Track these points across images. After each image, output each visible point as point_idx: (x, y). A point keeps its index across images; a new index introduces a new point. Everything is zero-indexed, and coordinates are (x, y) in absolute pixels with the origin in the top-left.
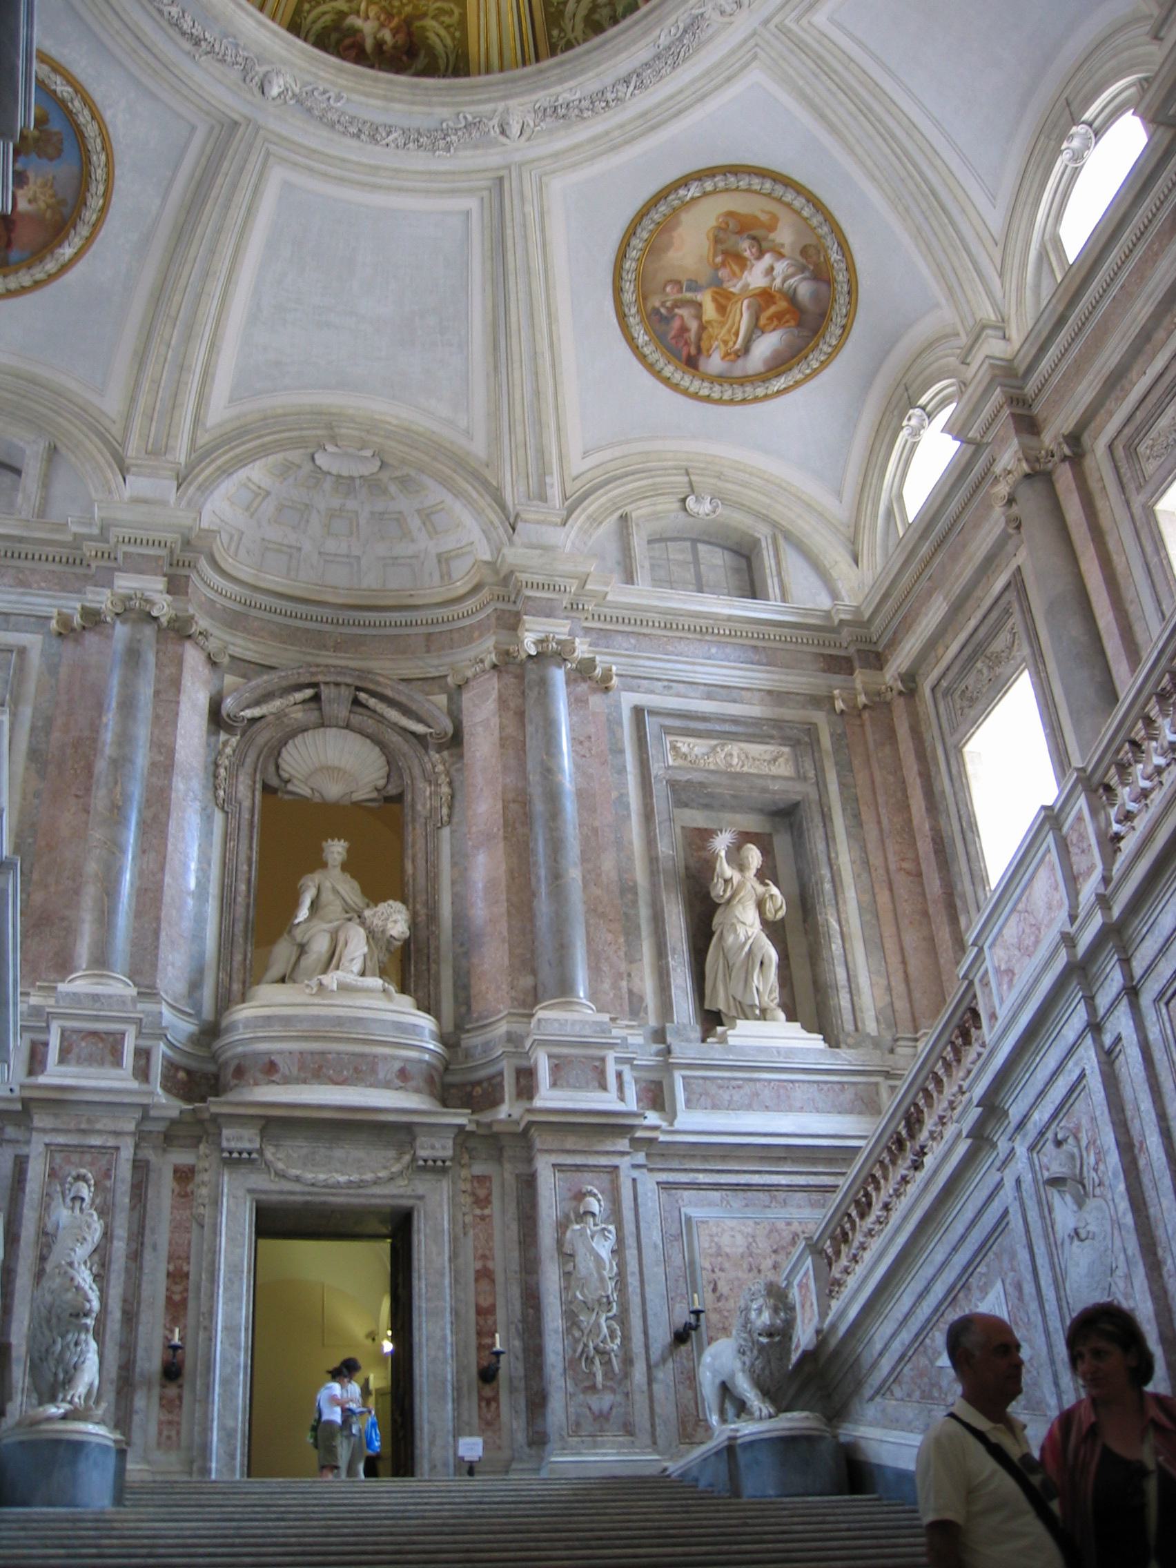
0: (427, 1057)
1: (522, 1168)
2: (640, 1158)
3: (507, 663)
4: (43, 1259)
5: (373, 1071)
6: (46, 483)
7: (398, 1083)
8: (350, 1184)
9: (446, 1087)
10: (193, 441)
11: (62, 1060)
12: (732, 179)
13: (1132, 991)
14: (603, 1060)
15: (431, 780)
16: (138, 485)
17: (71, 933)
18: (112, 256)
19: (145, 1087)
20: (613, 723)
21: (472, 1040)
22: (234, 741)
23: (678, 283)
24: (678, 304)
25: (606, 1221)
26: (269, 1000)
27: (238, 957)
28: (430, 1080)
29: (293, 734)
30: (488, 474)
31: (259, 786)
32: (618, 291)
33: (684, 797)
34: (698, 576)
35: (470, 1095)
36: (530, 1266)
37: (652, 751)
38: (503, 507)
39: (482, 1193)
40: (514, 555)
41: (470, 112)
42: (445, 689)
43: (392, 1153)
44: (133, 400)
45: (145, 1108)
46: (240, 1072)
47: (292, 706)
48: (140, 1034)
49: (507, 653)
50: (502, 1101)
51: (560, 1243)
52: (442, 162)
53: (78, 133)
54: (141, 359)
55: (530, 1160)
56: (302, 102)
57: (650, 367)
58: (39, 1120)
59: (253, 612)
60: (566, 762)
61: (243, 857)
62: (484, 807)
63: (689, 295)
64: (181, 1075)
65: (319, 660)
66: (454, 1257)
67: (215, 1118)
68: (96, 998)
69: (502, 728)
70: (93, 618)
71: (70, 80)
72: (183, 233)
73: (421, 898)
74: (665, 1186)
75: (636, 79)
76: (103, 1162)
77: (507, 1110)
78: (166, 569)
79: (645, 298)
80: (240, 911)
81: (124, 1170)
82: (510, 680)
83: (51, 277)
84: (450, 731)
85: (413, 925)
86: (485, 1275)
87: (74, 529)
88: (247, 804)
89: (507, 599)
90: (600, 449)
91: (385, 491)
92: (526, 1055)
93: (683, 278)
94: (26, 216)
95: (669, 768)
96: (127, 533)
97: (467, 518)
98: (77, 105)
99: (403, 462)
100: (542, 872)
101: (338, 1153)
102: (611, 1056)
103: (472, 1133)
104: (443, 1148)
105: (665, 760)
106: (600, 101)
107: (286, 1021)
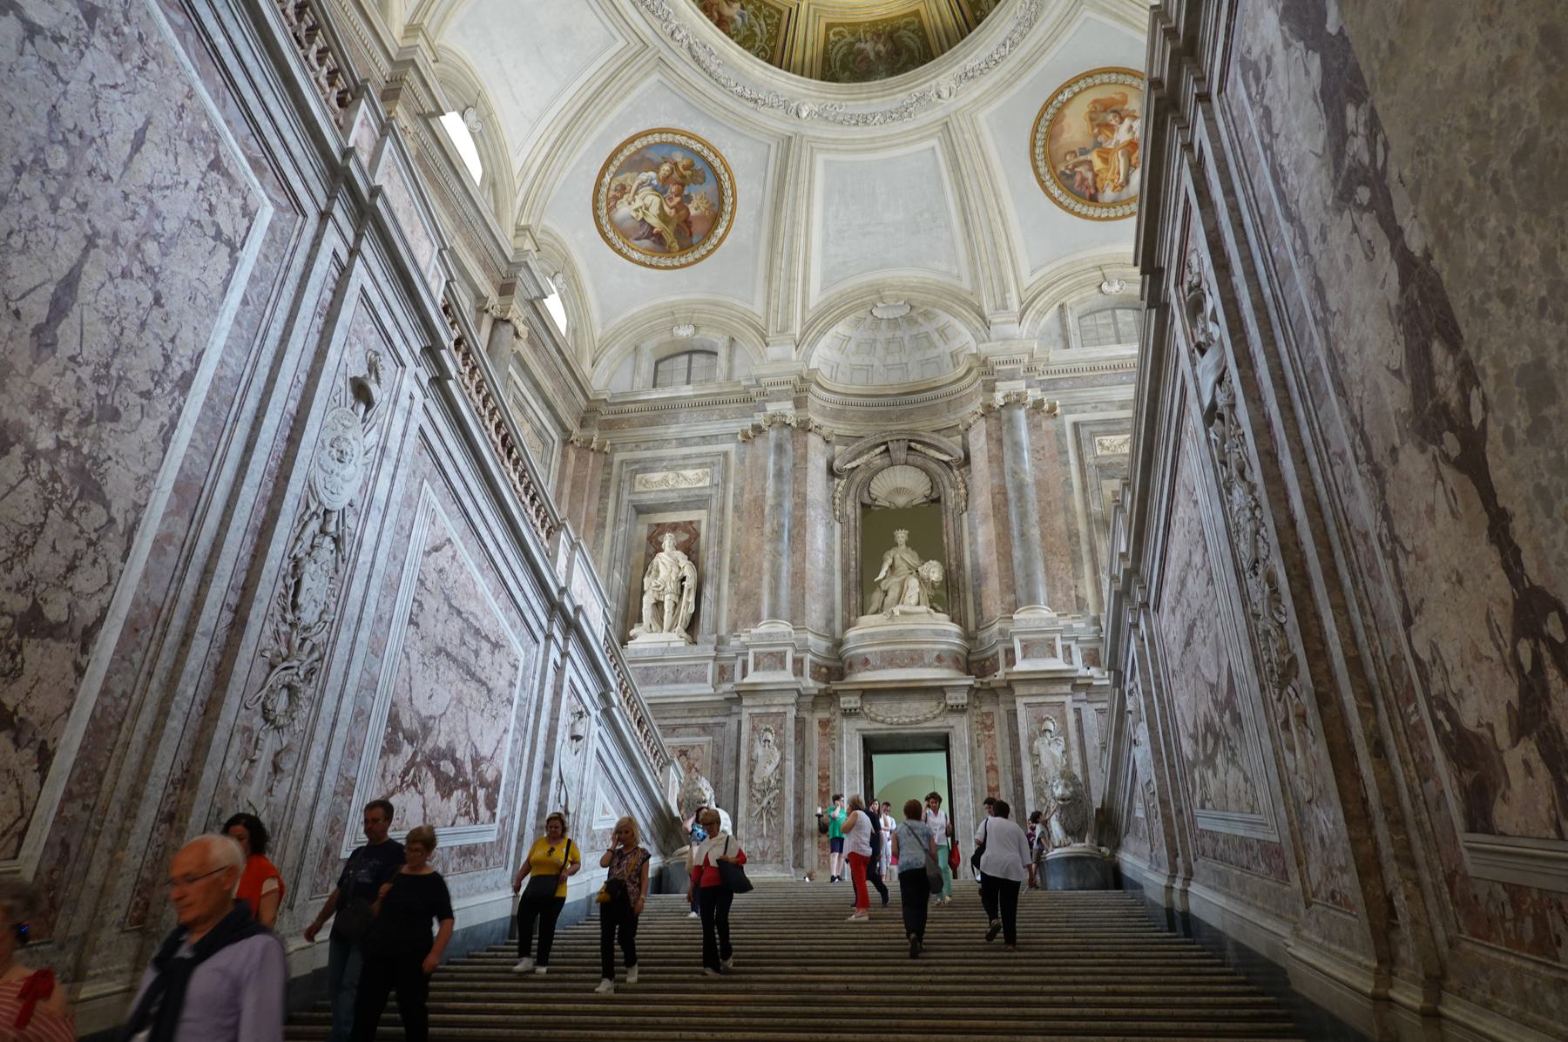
1: (1010, 707)
2: (1083, 695)
3: (989, 411)
4: (752, 773)
5: (922, 659)
6: (730, 359)
8: (911, 723)
11: (755, 669)
12: (1089, 80)
15: (954, 487)
16: (773, 352)
17: (759, 601)
20: (1060, 435)
21: (985, 635)
24: (1075, 166)
25: (1059, 734)
26: (868, 624)
28: (956, 661)
29: (877, 472)
30: (971, 298)
32: (1036, 168)
36: (1016, 763)
37: (1086, 448)
38: (983, 318)
39: (988, 722)
40: (985, 348)
41: (917, 91)
42: (959, 433)
43: (934, 703)
44: (768, 303)
46: (851, 666)
47: (875, 458)
51: (1031, 748)
52: (909, 125)
53: (710, 165)
54: (769, 279)
56: (821, 116)
57: (1066, 208)
60: (1027, 466)
62: (982, 500)
66: (972, 759)
67: (836, 692)
68: (770, 635)
69: (989, 451)
70: (758, 429)
71: (699, 140)
72: (777, 206)
73: (953, 556)
74: (1100, 711)
75: (1011, 43)
76: (779, 721)
77: (1000, 674)
80: (852, 576)
81: (790, 724)
82: (992, 421)
83: (716, 247)
85: (947, 574)
86: (992, 769)
90: (1041, 267)
92: (1011, 641)
97: (962, 328)
98: (706, 152)
99: (923, 303)
100: (1015, 533)
101: (905, 706)
102: (1058, 637)
103: (978, 690)
104: (962, 699)
106: (993, 62)
107: (872, 635)
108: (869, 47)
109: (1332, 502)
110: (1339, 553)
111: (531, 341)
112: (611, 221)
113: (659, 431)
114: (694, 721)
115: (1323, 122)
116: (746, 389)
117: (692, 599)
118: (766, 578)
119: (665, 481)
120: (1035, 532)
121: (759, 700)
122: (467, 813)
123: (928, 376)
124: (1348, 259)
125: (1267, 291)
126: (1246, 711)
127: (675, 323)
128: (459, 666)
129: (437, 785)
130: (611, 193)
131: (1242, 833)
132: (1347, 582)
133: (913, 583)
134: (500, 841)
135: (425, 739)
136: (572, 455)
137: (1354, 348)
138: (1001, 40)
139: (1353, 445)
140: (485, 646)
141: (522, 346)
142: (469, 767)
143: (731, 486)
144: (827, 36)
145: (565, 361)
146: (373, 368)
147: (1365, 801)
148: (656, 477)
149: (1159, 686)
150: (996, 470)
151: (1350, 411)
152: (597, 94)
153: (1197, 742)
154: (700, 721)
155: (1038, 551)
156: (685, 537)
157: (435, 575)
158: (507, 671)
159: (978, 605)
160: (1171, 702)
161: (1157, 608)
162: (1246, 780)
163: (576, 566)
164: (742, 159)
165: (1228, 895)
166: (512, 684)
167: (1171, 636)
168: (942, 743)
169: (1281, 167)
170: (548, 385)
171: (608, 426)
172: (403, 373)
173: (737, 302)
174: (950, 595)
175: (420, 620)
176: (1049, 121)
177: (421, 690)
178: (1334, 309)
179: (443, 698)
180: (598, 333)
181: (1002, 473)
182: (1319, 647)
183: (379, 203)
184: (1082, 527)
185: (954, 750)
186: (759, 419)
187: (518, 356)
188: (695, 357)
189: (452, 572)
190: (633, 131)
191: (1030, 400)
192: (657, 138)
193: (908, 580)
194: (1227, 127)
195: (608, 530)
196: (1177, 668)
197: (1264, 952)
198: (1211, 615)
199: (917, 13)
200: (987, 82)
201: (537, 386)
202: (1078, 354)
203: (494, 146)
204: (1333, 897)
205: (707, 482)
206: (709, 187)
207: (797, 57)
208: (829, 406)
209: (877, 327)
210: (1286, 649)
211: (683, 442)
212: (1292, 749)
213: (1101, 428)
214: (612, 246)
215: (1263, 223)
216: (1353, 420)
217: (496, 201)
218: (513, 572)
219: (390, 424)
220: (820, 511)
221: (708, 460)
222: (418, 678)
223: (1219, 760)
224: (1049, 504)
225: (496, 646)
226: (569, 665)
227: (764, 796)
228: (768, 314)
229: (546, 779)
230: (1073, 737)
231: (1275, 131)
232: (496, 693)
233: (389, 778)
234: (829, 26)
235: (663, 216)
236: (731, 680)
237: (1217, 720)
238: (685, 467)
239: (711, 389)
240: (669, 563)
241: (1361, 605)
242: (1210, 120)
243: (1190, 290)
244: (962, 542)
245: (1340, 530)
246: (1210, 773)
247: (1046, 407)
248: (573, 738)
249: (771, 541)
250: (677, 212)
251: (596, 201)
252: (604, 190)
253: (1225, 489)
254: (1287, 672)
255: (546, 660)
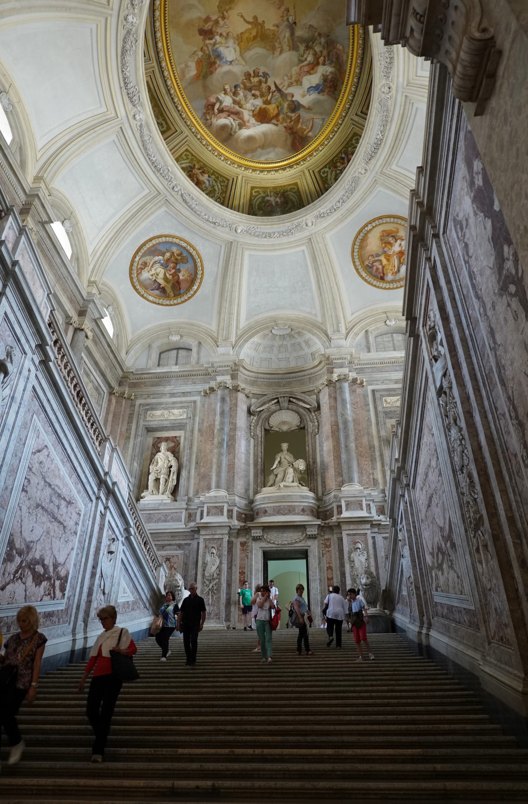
0: (311, 505)
1: (339, 536)
2: (376, 530)
3: (330, 383)
4: (204, 570)
5: (294, 510)
6: (198, 353)
7: (302, 513)
9: (318, 513)
10: (236, 333)
12: (380, 221)
13: (408, 485)
14: (362, 501)
16: (221, 350)
17: (210, 479)
18: (207, 286)
19: (231, 520)
20: (365, 396)
21: (326, 498)
22: (255, 418)
23: (372, 255)
24: (373, 262)
25: (364, 550)
26: (267, 492)
27: (259, 480)
30: (321, 326)
31: (263, 430)
32: (354, 262)
33: (390, 416)
34: (394, 345)
35: (326, 514)
36: (342, 565)
37: (378, 403)
38: (327, 336)
39: (328, 544)
40: (328, 351)
42: (315, 394)
43: (300, 534)
44: (219, 325)
45: (229, 526)
46: (257, 514)
47: (272, 406)
48: (229, 506)
49: (330, 381)
50: (333, 516)
52: (292, 238)
53: (191, 254)
54: (220, 313)
55: (341, 533)
57: (369, 283)
58: (202, 532)
59: (259, 380)
60: (349, 412)
61: (259, 451)
62: (326, 428)
63: (377, 258)
64: (243, 516)
65: (279, 391)
66: (319, 563)
68: (216, 497)
69: (330, 403)
70: (212, 390)
71: (185, 242)
73: (311, 457)
77: (334, 519)
78: (231, 372)
79: (363, 263)
80: (259, 467)
81: (225, 545)
82: (332, 388)
83: (193, 295)
84: (316, 406)
85: (308, 466)
86: (330, 568)
87: (205, 366)
88: (260, 436)
89: (329, 364)
90: (357, 311)
91: (294, 337)
92: (340, 501)
93: (374, 254)
94: (183, 280)
95: (384, 408)
96: (219, 364)
98: (189, 248)
100: (343, 446)
101: (285, 535)
102: (364, 499)
103: (323, 527)
104: (313, 531)
105: (382, 404)
106: (334, 210)
107: (269, 498)
108: (272, 199)
109: (499, 439)
110: (503, 464)
111: (94, 341)
112: (138, 280)
113: (160, 389)
114: (174, 542)
115: (493, 252)
116: (207, 369)
117: (175, 477)
118: (214, 467)
119: (163, 415)
120: (353, 445)
121: (209, 532)
122: (49, 594)
123: (299, 364)
124: (505, 320)
125: (467, 332)
126: (458, 541)
127: (170, 334)
128: (48, 514)
129: (33, 579)
130: (139, 266)
131: (456, 605)
132: (507, 479)
133: (291, 470)
134: (67, 609)
135: (28, 553)
136: (114, 401)
137: (509, 363)
138: (337, 199)
139: (509, 411)
140: (63, 503)
141: (89, 343)
142: (51, 569)
143: (197, 419)
144: (251, 193)
145: (112, 351)
146: (9, 355)
147: (517, 590)
148: (158, 413)
149: (415, 527)
150: (333, 413)
151: (508, 394)
152: (134, 216)
153: (433, 557)
154: (177, 542)
155: (354, 455)
156: (172, 444)
157: (37, 465)
158: (75, 516)
159: (324, 482)
160: (421, 535)
161: (414, 487)
162: (458, 577)
163: (114, 461)
164: (208, 253)
165: (450, 637)
166: (77, 524)
167: (421, 502)
168: (304, 554)
169: (473, 272)
170: (102, 364)
171: (134, 385)
172: (25, 357)
173: (203, 324)
174: (309, 477)
175: (28, 489)
176: (360, 240)
177: (27, 526)
178: (499, 343)
179: (39, 531)
180: (130, 337)
181: (336, 415)
182: (494, 511)
183: (17, 269)
184: (376, 443)
185: (309, 558)
186: (213, 384)
187: (87, 349)
188: (180, 351)
189: (47, 464)
190: (151, 235)
191: (351, 378)
192: (164, 239)
193: (288, 470)
194: (447, 251)
195: (132, 440)
196: (423, 518)
197: (468, 668)
198: (441, 492)
199: (296, 184)
200: (330, 220)
201: (96, 364)
202: (374, 355)
203: (78, 239)
204: (502, 640)
205: (185, 416)
206: (190, 265)
207: (236, 202)
208: (249, 378)
209: (274, 339)
210: (477, 511)
211: (173, 395)
212: (481, 562)
213: (386, 393)
214: (139, 293)
215: (465, 298)
216: (509, 398)
217: (78, 268)
218: (80, 464)
219: (17, 384)
220: (243, 432)
221: (186, 405)
222: (25, 521)
223: (445, 566)
224: (360, 431)
225: (69, 503)
226: (108, 513)
227: (210, 583)
228: (218, 330)
229: (93, 575)
230: (371, 551)
231: (470, 254)
232: (68, 528)
233: (6, 575)
234: (252, 188)
235: (166, 279)
236: (195, 520)
237: (443, 545)
238: (174, 408)
239: (188, 368)
240: (163, 458)
241: (514, 491)
242: (439, 247)
243: (430, 329)
244: (315, 449)
245: (503, 452)
246: (440, 573)
247: (359, 382)
248: (109, 552)
249: (217, 447)
250: (173, 277)
251: (131, 269)
252: (135, 264)
253: (447, 429)
254: (478, 523)
255: (96, 511)
